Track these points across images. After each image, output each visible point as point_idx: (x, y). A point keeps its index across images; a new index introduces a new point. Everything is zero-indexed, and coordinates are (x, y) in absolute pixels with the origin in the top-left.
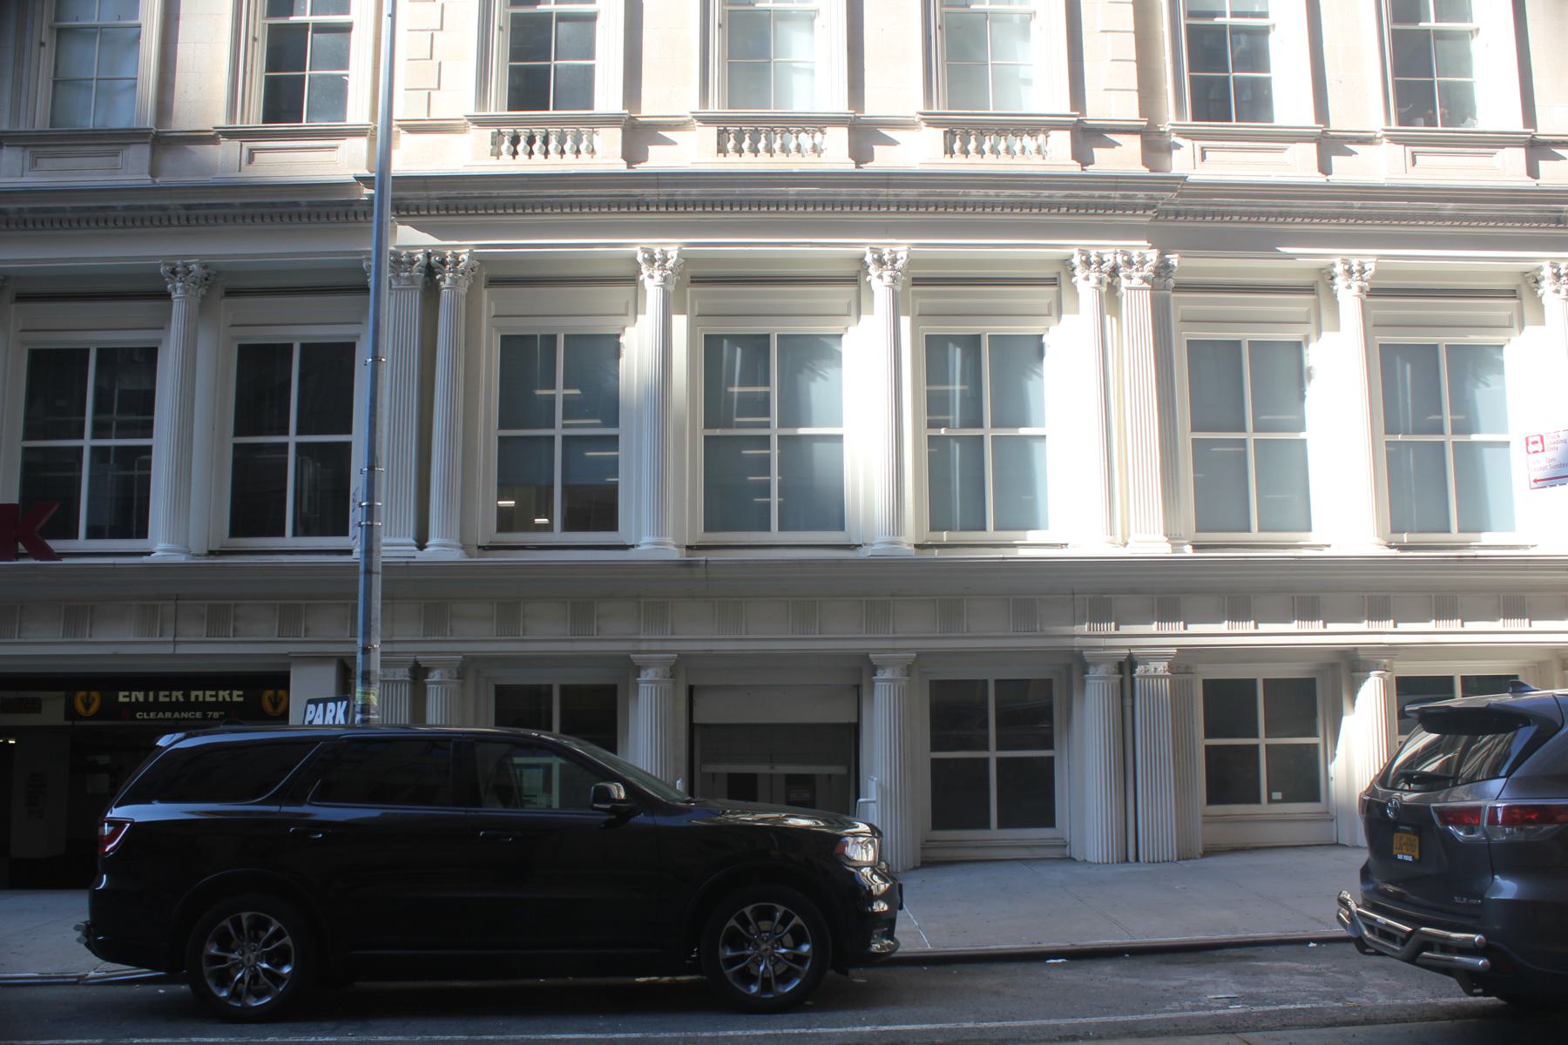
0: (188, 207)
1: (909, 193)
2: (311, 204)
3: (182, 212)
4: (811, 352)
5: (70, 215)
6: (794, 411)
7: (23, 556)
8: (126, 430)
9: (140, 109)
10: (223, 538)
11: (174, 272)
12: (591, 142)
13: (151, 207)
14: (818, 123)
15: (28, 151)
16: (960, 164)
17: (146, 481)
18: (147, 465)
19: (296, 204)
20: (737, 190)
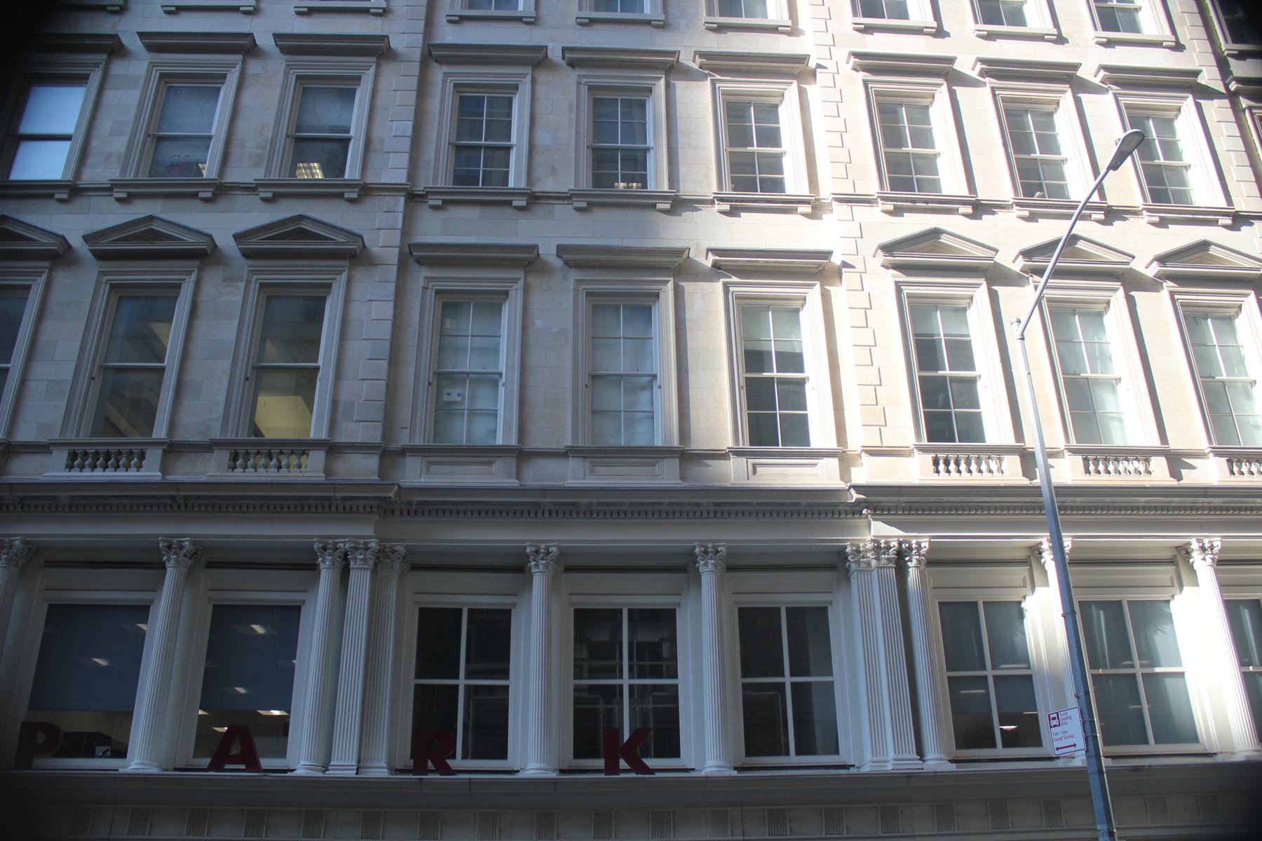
0: (717, 505)
1: (1218, 501)
2: (809, 505)
3: (712, 508)
4: (1152, 614)
5: (626, 508)
6: (1150, 657)
7: (432, 772)
8: (657, 673)
9: (665, 433)
10: (569, 761)
11: (706, 552)
12: (988, 464)
13: (689, 504)
14: (1000, 451)
15: (587, 462)
16: (943, 479)
17: (675, 713)
18: (675, 699)
19: (798, 504)
20: (1107, 499)
